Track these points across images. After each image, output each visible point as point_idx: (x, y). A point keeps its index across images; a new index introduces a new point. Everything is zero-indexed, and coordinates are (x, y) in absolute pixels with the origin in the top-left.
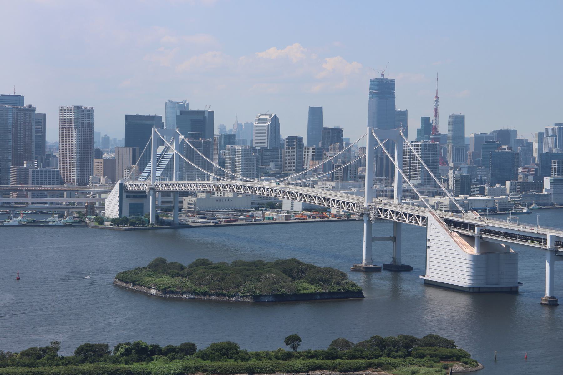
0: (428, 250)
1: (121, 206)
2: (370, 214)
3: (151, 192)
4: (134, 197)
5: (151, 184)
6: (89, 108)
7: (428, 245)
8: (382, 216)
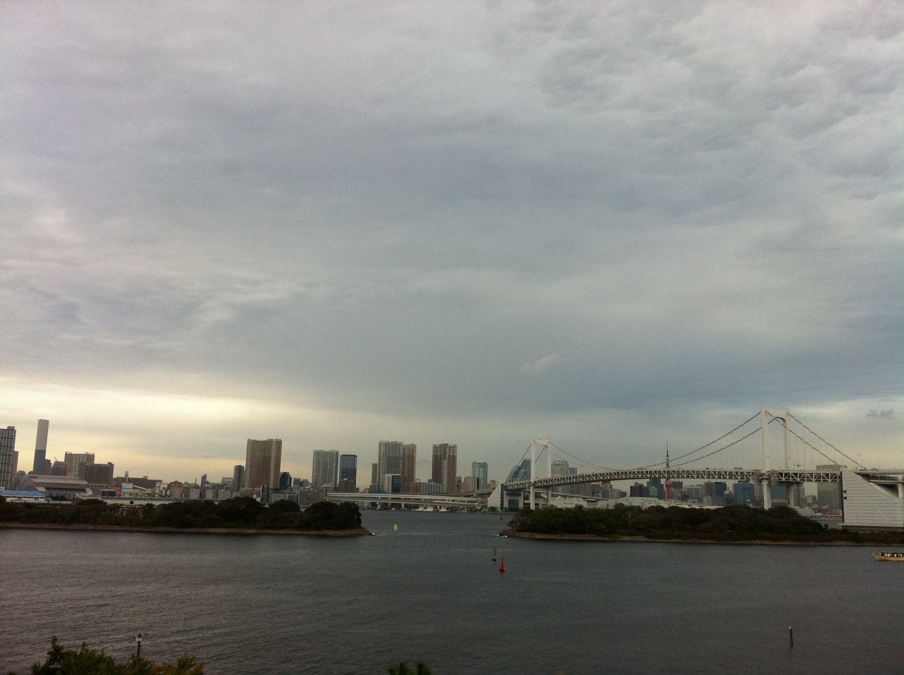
0: (845, 501)
1: (502, 501)
3: (531, 488)
5: (531, 481)
8: (784, 479)
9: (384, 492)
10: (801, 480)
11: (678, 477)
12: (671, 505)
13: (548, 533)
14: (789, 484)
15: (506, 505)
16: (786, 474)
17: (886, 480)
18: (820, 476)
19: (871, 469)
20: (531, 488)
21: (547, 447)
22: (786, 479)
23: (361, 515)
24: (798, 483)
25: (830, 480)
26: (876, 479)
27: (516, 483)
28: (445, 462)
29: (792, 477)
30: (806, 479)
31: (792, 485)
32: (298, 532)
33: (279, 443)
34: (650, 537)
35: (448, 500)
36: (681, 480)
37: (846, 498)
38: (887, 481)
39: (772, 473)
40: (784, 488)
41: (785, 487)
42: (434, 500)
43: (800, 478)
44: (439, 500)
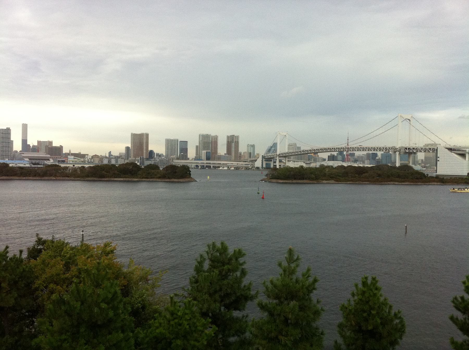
0: (438, 162)
2: (400, 151)
4: (267, 161)
6: (237, 136)
7: (438, 160)
8: (407, 151)
9: (202, 160)
10: (416, 151)
11: (353, 151)
12: (348, 165)
13: (285, 179)
14: (410, 153)
15: (264, 166)
16: (409, 149)
17: (460, 151)
18: (426, 149)
19: (453, 146)
20: (277, 157)
21: (286, 136)
22: (409, 151)
23: (191, 172)
24: (415, 153)
25: (431, 151)
26: (455, 151)
27: (269, 155)
28: (233, 145)
29: (412, 150)
30: (419, 151)
31: (412, 154)
32: (159, 180)
33: (147, 135)
34: (337, 181)
35: (235, 164)
36: (354, 152)
37: (439, 161)
38: (461, 152)
39: (402, 147)
40: (407, 155)
41: (408, 155)
42: (227, 164)
43: (416, 150)
44: (230, 164)
